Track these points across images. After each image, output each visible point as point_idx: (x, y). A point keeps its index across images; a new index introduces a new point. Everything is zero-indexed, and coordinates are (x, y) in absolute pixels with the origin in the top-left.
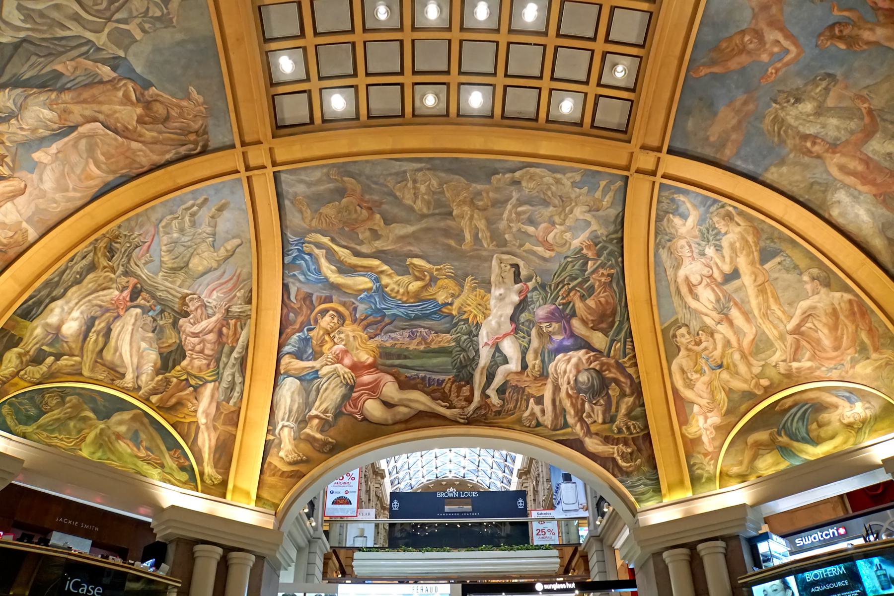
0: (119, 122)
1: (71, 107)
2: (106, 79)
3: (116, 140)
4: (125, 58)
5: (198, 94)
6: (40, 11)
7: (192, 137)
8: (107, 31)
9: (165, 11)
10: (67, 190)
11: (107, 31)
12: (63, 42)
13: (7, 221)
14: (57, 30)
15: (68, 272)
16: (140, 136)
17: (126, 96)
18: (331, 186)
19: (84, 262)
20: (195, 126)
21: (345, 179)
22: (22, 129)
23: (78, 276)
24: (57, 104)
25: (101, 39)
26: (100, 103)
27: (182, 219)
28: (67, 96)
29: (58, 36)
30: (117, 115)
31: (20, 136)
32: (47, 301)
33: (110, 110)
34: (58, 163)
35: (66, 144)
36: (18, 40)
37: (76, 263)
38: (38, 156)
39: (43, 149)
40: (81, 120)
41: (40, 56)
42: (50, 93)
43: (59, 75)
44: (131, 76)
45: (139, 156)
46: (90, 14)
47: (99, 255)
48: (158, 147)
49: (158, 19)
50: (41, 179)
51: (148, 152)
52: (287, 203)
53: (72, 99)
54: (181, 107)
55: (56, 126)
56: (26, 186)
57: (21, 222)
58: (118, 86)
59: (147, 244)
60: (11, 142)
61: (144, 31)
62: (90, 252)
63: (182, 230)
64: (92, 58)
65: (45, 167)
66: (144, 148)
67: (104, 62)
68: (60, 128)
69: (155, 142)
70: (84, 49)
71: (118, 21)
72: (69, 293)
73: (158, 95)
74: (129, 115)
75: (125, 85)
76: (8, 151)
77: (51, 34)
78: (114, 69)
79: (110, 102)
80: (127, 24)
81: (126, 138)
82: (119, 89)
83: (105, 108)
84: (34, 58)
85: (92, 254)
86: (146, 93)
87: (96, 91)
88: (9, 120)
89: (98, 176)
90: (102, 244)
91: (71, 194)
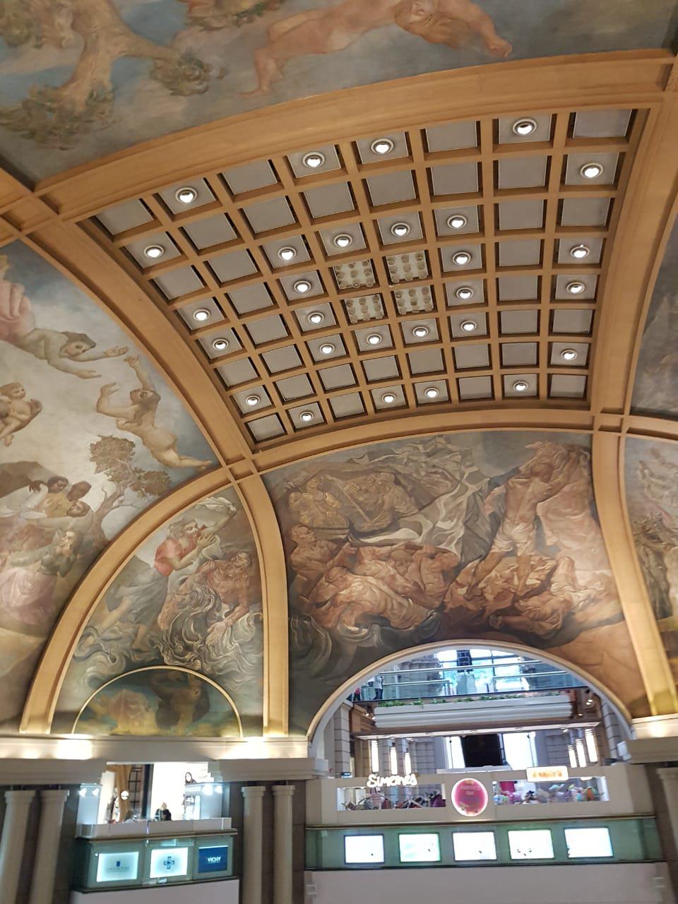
2: (505, 491)
5: (534, 443)
6: (447, 513)
7: (574, 455)
9: (458, 453)
10: (585, 538)
12: (471, 506)
13: (588, 579)
14: (461, 507)
15: (652, 571)
16: (559, 483)
18: (667, 375)
19: (652, 557)
20: (564, 451)
21: (663, 361)
22: (525, 543)
23: (660, 567)
25: (473, 488)
26: (522, 498)
27: (652, 483)
28: (510, 514)
32: (665, 596)
37: (649, 562)
38: (549, 542)
39: (546, 537)
40: (531, 512)
41: (478, 519)
43: (493, 515)
44: (507, 478)
46: (452, 491)
47: (651, 545)
49: (463, 457)
50: (568, 548)
51: (575, 484)
52: (674, 410)
54: (543, 456)
56: (568, 557)
57: (594, 574)
59: (663, 513)
60: (532, 551)
61: (472, 466)
62: (644, 549)
63: (664, 487)
68: (534, 524)
69: (568, 477)
70: (478, 497)
72: (670, 580)
73: (527, 466)
74: (537, 485)
75: (513, 483)
76: (538, 556)
78: (498, 486)
80: (464, 474)
81: (557, 493)
82: (514, 487)
83: (527, 497)
84: (477, 523)
85: (648, 550)
86: (523, 473)
87: (511, 497)
88: (517, 548)
89: (582, 517)
90: (644, 540)
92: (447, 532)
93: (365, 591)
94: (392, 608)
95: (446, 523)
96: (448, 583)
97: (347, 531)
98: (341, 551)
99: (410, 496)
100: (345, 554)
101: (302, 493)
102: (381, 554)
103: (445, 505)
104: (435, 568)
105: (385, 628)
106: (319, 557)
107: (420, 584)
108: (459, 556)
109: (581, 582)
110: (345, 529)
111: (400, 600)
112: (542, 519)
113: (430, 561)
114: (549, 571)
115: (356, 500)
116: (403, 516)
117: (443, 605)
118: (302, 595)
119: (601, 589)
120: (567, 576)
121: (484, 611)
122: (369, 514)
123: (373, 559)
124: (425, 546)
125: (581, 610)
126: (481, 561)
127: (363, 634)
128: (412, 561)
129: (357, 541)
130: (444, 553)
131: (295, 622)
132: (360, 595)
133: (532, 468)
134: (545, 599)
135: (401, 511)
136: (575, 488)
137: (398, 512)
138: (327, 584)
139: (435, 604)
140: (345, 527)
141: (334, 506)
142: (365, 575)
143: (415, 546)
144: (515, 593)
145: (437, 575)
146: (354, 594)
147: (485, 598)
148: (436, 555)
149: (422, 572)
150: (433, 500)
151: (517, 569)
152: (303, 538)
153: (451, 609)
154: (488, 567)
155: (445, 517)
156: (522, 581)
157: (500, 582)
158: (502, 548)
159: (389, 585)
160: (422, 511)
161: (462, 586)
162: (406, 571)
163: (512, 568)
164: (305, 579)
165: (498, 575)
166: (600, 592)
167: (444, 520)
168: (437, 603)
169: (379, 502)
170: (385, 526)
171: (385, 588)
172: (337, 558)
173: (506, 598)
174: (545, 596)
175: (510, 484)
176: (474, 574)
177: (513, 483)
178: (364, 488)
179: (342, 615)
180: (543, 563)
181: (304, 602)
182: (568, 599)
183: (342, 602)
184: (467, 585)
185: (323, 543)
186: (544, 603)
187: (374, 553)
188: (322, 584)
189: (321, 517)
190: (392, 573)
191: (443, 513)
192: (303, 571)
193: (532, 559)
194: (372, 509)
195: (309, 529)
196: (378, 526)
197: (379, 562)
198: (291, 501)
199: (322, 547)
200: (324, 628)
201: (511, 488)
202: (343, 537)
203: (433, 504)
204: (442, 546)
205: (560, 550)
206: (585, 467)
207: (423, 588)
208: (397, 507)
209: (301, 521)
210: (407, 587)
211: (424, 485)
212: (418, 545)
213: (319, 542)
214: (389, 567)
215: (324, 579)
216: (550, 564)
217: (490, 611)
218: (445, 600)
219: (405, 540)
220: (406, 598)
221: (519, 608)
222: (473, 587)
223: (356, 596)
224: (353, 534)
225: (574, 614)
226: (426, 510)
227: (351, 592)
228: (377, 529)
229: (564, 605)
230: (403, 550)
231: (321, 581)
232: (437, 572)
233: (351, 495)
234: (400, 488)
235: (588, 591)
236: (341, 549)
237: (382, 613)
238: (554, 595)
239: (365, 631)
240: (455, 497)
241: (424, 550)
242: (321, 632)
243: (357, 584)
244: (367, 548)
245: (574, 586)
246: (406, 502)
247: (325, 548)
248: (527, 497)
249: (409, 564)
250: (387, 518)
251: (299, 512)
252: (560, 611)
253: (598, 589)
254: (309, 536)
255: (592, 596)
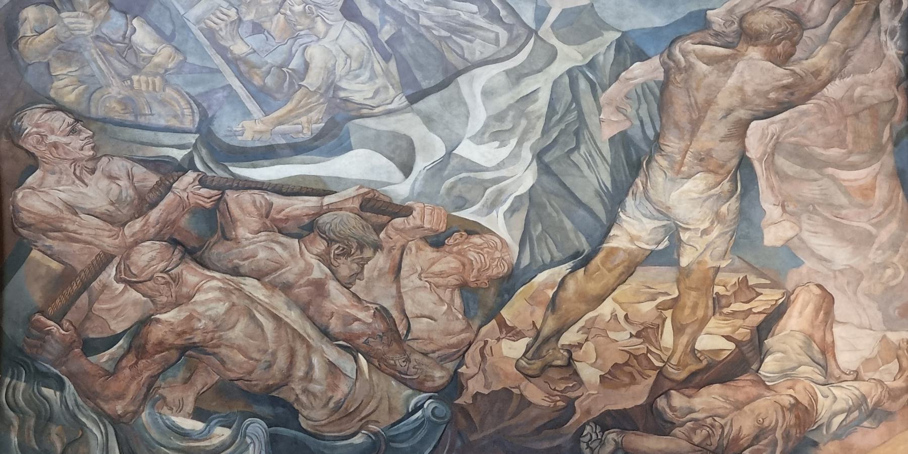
0: (768, 92)
1: (696, 147)
2: (661, 77)
3: (804, 113)
4: (624, 34)
6: (489, 117)
8: (554, 41)
11: (554, 41)
12: (560, 108)
13: (867, 354)
14: (531, 108)
16: (816, 73)
17: (711, 61)
22: (705, 232)
24: (682, 164)
26: (709, 103)
28: (673, 144)
29: (545, 110)
30: (749, 89)
31: (719, 242)
33: (732, 94)
34: (804, 217)
35: (772, 188)
36: (535, 163)
39: (763, 223)
40: (732, 145)
41: (577, 148)
42: (654, 163)
43: (622, 141)
45: (862, 96)
48: (857, 57)
50: (821, 259)
51: (861, 78)
53: (681, 138)
55: (726, 185)
57: (884, 337)
58: (683, 63)
60: (723, 257)
64: (606, 81)
65: (802, 240)
66: (848, 80)
67: (620, 66)
68: (734, 180)
70: (583, 85)
71: (540, 19)
73: (731, 11)
75: (685, 54)
76: (735, 271)
77: (539, 118)
78: (642, 56)
79: (715, 90)
80: (549, 10)
82: (690, 67)
83: (724, 100)
84: (575, 157)
86: (716, 27)
87: (679, 99)
88: (680, 240)
91: (884, 235)
92: (488, 176)
93: (234, 319)
94: (308, 376)
95: (483, 148)
96: (475, 324)
97: (192, 139)
98: (170, 196)
99: (387, 58)
100: (182, 205)
101: (59, 11)
102: (287, 219)
103: (488, 94)
104: (440, 274)
105: (282, 430)
106: (101, 203)
107: (395, 314)
108: (516, 249)
109: (846, 359)
110: (184, 132)
111: (332, 353)
112: (759, 168)
113: (429, 253)
114: (762, 317)
115: (223, 51)
116: (359, 112)
117: (456, 384)
118: (42, 312)
119: (900, 383)
120: (810, 337)
121: (570, 408)
122: (262, 96)
123: (266, 229)
124: (418, 207)
125: (837, 436)
126: (574, 270)
127: (216, 441)
128: (377, 247)
129: (221, 173)
130: (470, 233)
131: (14, 389)
132: (218, 328)
133: (742, 19)
134: (741, 396)
135: (357, 98)
136: (858, 91)
137: (346, 100)
138: (121, 286)
139: (433, 379)
140: (188, 124)
141: (157, 60)
142: (236, 272)
143: (391, 204)
144: (661, 372)
145: (446, 295)
146: (200, 325)
147: (576, 373)
148: (450, 235)
149: (404, 282)
150: (450, 77)
151: (674, 304)
152: (55, 145)
153: (476, 396)
154: (594, 288)
155: (482, 132)
156: (684, 339)
157: (623, 336)
158: (639, 238)
159: (304, 309)
160: (415, 106)
161: (514, 333)
162: (358, 275)
163: (661, 299)
164: (55, 265)
165: (621, 314)
166: (893, 395)
167: (478, 138)
168: (439, 376)
169: (293, 64)
170: (307, 135)
171: (293, 317)
172: (155, 214)
173: (633, 381)
174: (744, 387)
175: (677, 52)
176: (553, 305)
177: (685, 54)
178: (249, 17)
179: (157, 384)
180: (745, 290)
181: (49, 332)
182: (805, 401)
183: (160, 343)
184: (533, 333)
185: (119, 166)
186: (739, 406)
187: (266, 213)
188: (105, 287)
189: (116, 89)
190: (316, 274)
191: (479, 116)
192: (49, 242)
193: (720, 277)
194: (269, 81)
195: (77, 120)
196: (284, 134)
197: (283, 239)
198: (26, 30)
199: (112, 178)
200: (102, 414)
201: (679, 70)
202: (179, 155)
203: (445, 92)
204: (465, 214)
205: (799, 263)
206: (892, 33)
207: (402, 329)
208: (343, 84)
209: (52, 94)
210: (357, 320)
211: (428, 28)
212: (395, 202)
213: (105, 160)
214: (308, 255)
215: (114, 273)
216: (769, 298)
217: (588, 412)
218: (463, 370)
219: (361, 184)
220: (351, 349)
221: (670, 414)
222: (547, 340)
223: (205, 331)
224: (212, 151)
225: (815, 444)
226: (431, 103)
227: (190, 318)
228: (283, 142)
229: (791, 418)
230: (351, 210)
231: (103, 277)
232: (446, 287)
233: (211, 34)
234: (359, 31)
235: (864, 387)
236: (169, 189)
237: (278, 387)
238: (768, 388)
239: (221, 434)
240: (517, 76)
241: (413, 221)
242: (89, 424)
243: (211, 295)
244: (246, 196)
245: (825, 368)
246: (373, 77)
247: (124, 183)
248: (724, 100)
249: (368, 253)
250: (314, 115)
251: (48, 65)
252: (779, 434)
253: (890, 384)
254: (76, 142)
255: (871, 403)
